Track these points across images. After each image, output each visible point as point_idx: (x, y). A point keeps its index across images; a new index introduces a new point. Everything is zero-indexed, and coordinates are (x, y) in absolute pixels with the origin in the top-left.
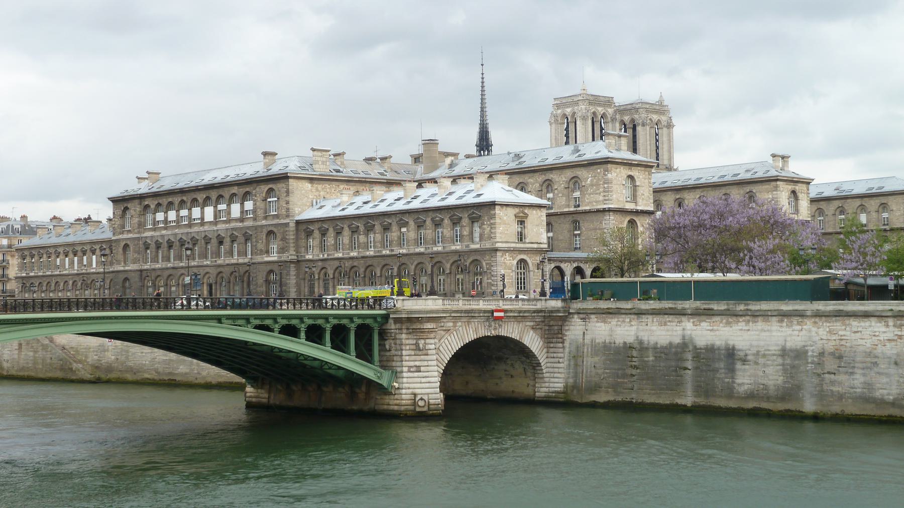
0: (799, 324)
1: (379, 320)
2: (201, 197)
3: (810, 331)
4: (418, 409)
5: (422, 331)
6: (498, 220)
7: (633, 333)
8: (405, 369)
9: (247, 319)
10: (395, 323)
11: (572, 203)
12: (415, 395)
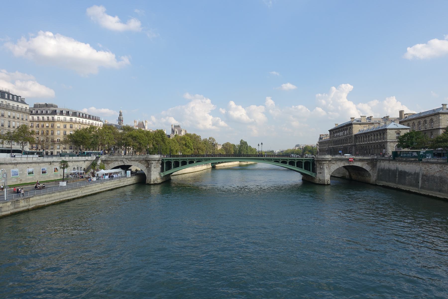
0: (419, 165)
1: (311, 160)
2: (341, 129)
3: (421, 168)
4: (320, 183)
5: (321, 163)
6: (388, 134)
7: (388, 166)
8: (318, 173)
9: (271, 159)
10: (316, 161)
11: (431, 127)
12: (320, 179)
